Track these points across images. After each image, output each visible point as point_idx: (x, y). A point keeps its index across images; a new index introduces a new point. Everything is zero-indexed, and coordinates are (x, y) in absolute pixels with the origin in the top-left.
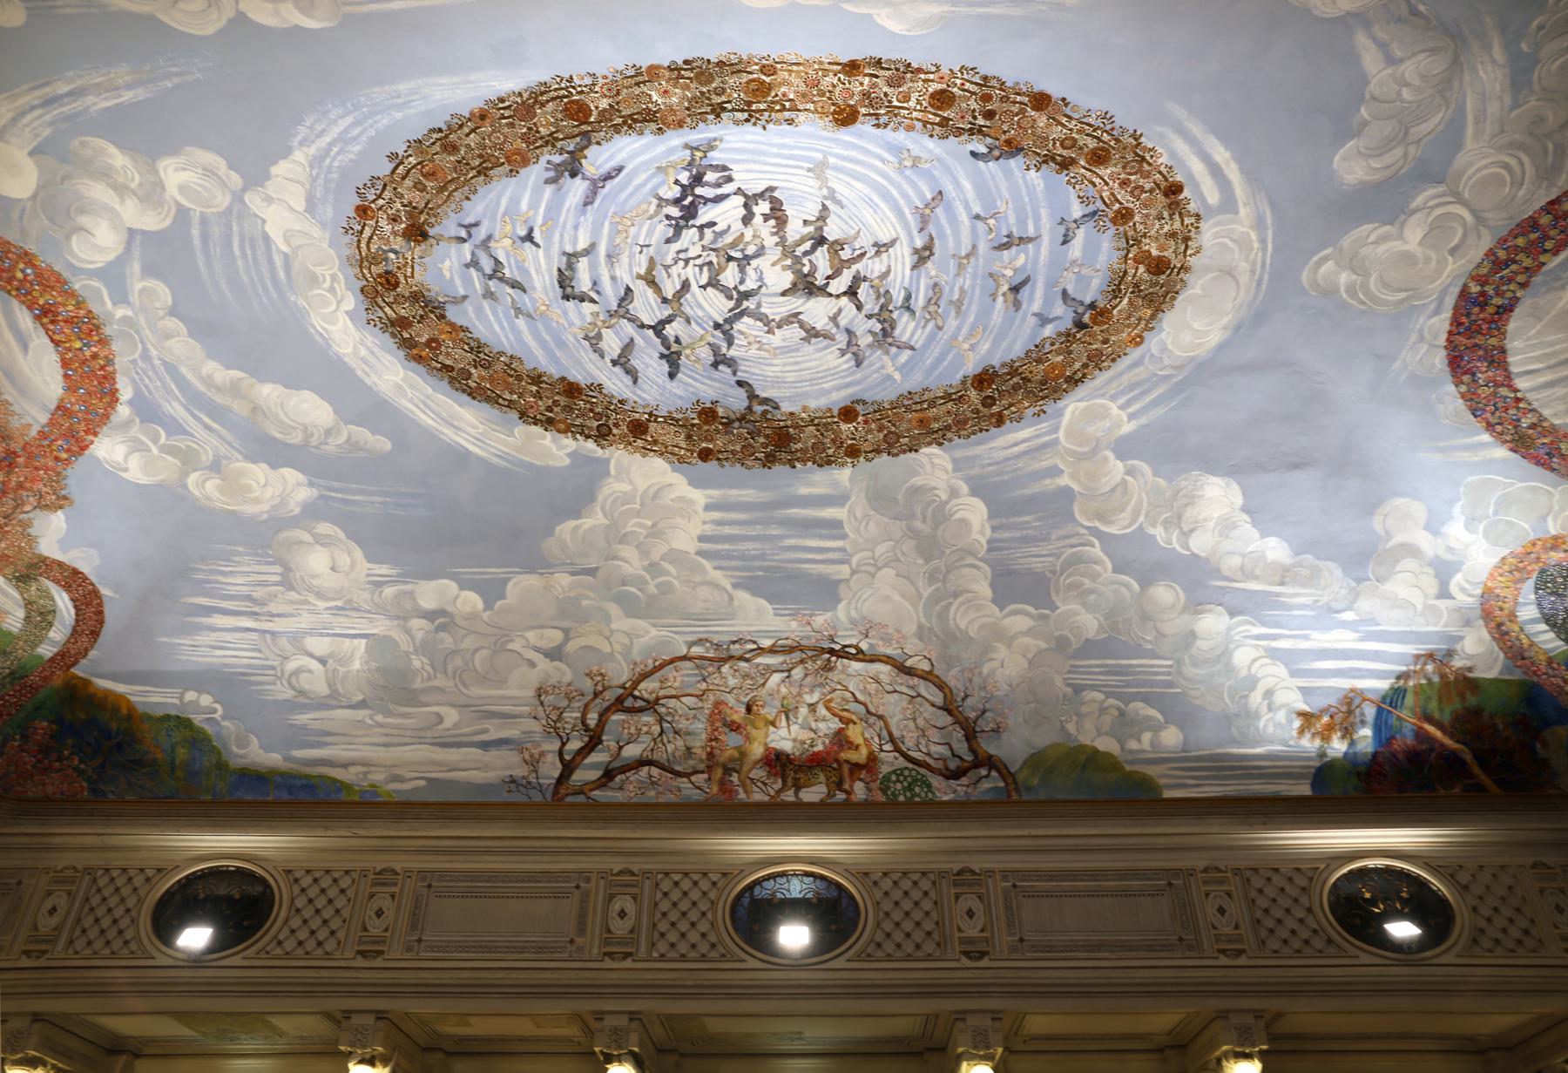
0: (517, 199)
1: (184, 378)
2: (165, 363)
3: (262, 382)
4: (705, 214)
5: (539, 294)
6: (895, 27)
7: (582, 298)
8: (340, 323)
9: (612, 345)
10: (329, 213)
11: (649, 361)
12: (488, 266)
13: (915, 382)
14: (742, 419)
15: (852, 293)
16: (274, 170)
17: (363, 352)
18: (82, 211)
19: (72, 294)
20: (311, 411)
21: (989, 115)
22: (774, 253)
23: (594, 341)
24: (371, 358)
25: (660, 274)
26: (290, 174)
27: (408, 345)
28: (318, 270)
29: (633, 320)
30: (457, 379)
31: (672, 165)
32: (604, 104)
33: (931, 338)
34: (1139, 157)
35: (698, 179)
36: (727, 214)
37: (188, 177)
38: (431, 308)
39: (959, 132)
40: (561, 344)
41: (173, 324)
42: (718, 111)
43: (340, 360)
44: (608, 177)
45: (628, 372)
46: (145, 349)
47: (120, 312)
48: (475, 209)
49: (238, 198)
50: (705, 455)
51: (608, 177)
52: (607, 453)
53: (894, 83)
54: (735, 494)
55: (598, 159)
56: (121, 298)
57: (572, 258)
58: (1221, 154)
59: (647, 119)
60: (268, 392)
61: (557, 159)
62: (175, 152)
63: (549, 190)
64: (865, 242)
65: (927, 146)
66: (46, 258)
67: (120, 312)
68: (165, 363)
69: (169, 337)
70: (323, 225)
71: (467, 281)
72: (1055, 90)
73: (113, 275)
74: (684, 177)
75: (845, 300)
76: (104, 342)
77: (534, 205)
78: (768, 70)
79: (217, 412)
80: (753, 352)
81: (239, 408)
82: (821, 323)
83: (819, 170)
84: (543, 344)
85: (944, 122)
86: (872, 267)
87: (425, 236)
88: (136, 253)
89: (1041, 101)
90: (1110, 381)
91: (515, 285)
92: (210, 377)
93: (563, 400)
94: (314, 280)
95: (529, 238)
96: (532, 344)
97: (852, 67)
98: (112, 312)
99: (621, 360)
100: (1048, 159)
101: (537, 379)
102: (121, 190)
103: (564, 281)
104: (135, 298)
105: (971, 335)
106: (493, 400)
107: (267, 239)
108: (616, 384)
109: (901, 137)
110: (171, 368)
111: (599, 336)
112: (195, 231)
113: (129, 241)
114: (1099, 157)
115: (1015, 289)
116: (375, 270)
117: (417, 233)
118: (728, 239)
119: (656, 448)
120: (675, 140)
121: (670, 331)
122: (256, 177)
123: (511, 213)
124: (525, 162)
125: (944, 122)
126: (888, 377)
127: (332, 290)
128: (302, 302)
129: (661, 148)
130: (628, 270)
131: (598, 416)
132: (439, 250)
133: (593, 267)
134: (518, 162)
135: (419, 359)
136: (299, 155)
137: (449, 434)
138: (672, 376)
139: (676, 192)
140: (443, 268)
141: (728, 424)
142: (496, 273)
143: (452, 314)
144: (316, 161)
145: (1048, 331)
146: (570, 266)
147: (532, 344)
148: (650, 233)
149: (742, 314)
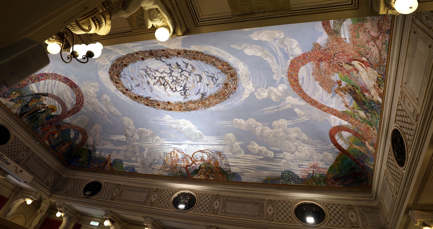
0: (211, 90)
1: (276, 60)
2: (279, 64)
3: (260, 56)
4: (182, 88)
5: (204, 75)
6: (168, 116)
7: (197, 75)
8: (241, 68)
9: (190, 67)
10: (241, 88)
11: (183, 66)
12: (214, 79)
13: (136, 64)
14: (160, 57)
15: (155, 77)
16: (248, 96)
17: (237, 64)
18: (283, 92)
19: (290, 82)
20: (249, 52)
21: (152, 103)
22: (170, 82)
23: (193, 68)
24: (236, 63)
25: (185, 78)
26: (246, 96)
27: (228, 65)
28: (245, 77)
29: (187, 72)
30: (218, 59)
31: (189, 95)
32: (200, 105)
33: (139, 71)
34: (131, 97)
35: (185, 93)
36: (179, 89)
37: (263, 94)
38: (223, 71)
39: (154, 101)
40: (199, 66)
41: (274, 72)
42: (185, 104)
43: (242, 61)
44: (197, 93)
45: (185, 63)
46: (282, 68)
47: (284, 76)
48: (217, 89)
49: (256, 90)
50: (163, 50)
51: (197, 93)
52: (183, 48)
53: (165, 107)
54: (154, 45)
55: (199, 97)
56: (282, 78)
57: (200, 81)
58: (122, 98)
59: (194, 102)
60: (259, 54)
61: (205, 96)
62: (264, 99)
63: (206, 91)
64: (158, 85)
65: (157, 99)
66: (291, 89)
67: (284, 76)
68: (279, 64)
69: (276, 69)
70: (242, 86)
71: (218, 76)
72: (146, 106)
73: (282, 82)
74: (187, 93)
75: (155, 76)
76: (288, 72)
77: (208, 90)
78: (180, 110)
79: (271, 51)
80: (165, 67)
81: (267, 51)
82: (157, 73)
83: (169, 95)
84: (202, 67)
85: (157, 102)
86: (154, 81)
87: (225, 84)
88: (276, 84)
89: (147, 105)
90: (107, 67)
91: (209, 76)
92: (271, 59)
93: (195, 57)
94: (246, 76)
95: (208, 85)
96: (204, 66)
97: (171, 110)
98: (285, 77)
99: (187, 65)
100: (141, 97)
101: (202, 60)
102: (275, 93)
103: (201, 78)
104: (280, 77)
105: (133, 71)
106: (209, 56)
107: (253, 83)
108: (187, 61)
109: (161, 100)
110: (278, 63)
111: (192, 69)
112: (265, 85)
113: (277, 86)
114: (136, 98)
115: (132, 79)
116: (234, 78)
117: (226, 84)
118: (177, 85)
119: (175, 50)
120: (189, 99)
121: (180, 70)
122: (252, 95)
123: (211, 89)
124: (210, 96)
125: (157, 102)
126: (140, 65)
127: (243, 74)
128: (249, 72)
129: (191, 98)
130: (191, 79)
131: (188, 55)
132: (223, 82)
133: (197, 79)
134: (211, 96)
135: (226, 63)
136: (243, 99)
137: (218, 49)
138: (177, 63)
139: (187, 91)
140: (222, 78)
141: (162, 56)
142: (213, 78)
143: (220, 71)
144: (241, 98)
145: (123, 73)
146: (200, 80)
147: (204, 66)
148: (189, 85)
149: (170, 73)
